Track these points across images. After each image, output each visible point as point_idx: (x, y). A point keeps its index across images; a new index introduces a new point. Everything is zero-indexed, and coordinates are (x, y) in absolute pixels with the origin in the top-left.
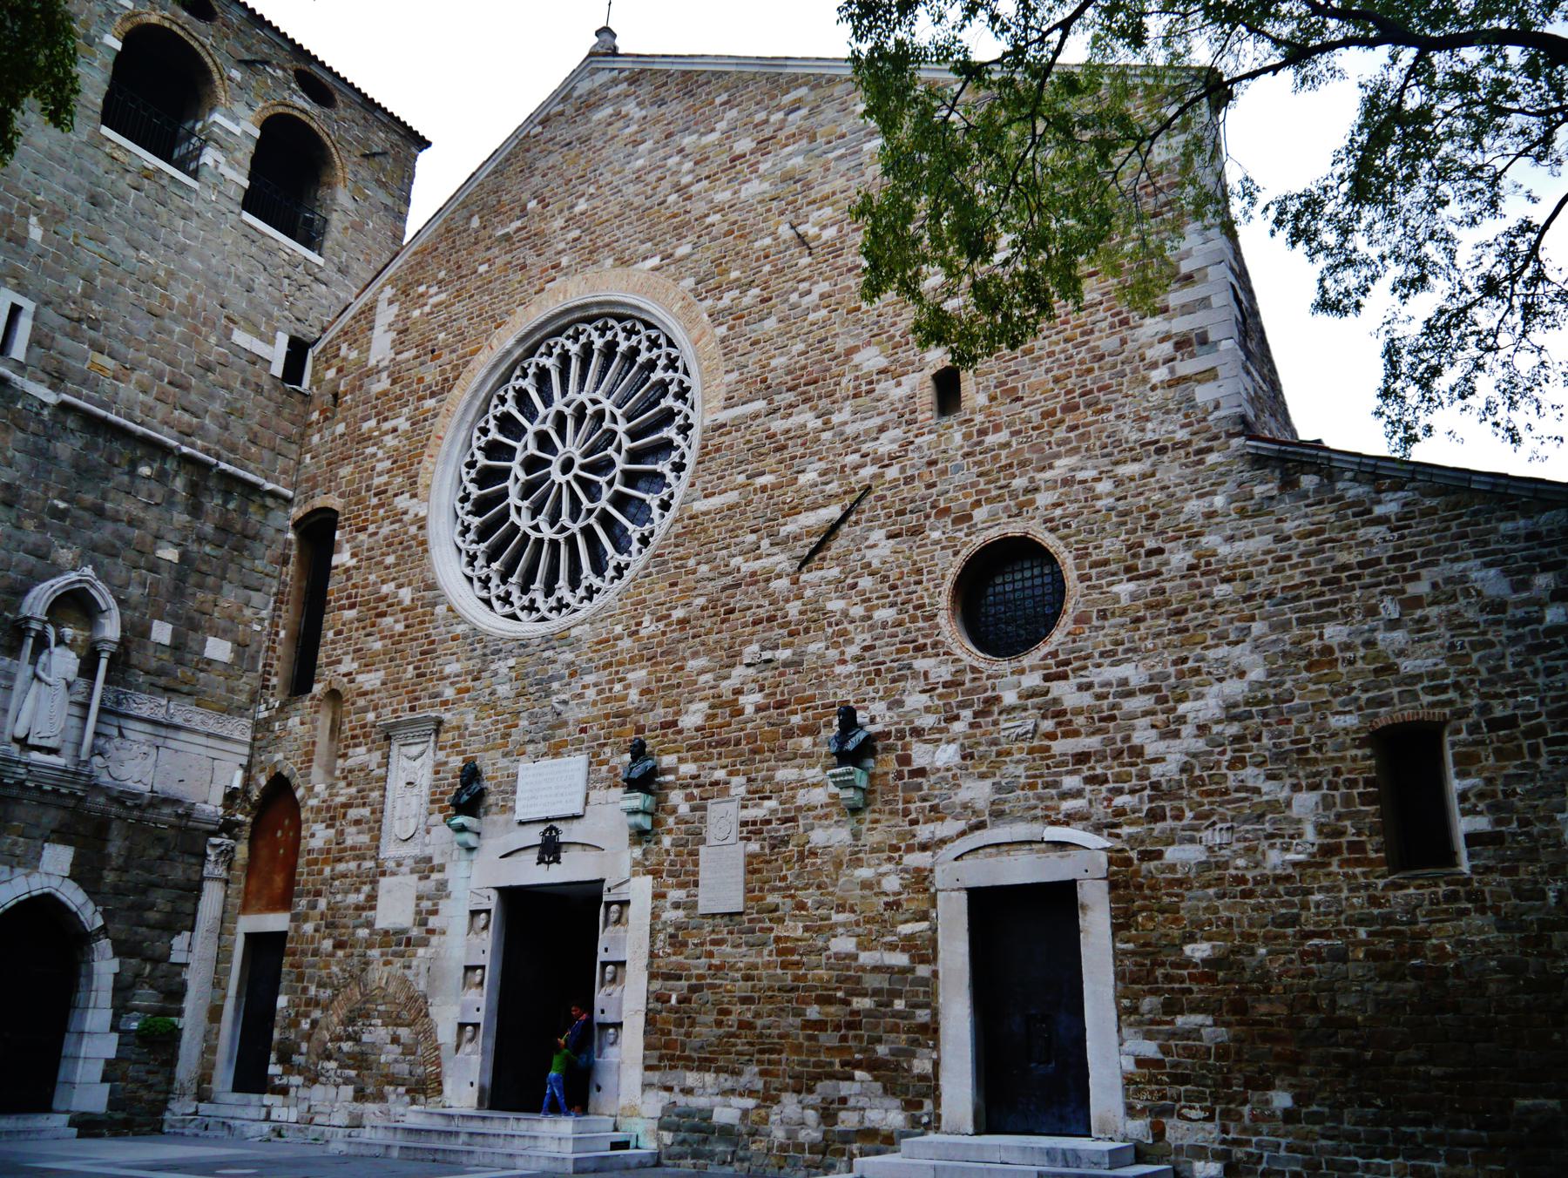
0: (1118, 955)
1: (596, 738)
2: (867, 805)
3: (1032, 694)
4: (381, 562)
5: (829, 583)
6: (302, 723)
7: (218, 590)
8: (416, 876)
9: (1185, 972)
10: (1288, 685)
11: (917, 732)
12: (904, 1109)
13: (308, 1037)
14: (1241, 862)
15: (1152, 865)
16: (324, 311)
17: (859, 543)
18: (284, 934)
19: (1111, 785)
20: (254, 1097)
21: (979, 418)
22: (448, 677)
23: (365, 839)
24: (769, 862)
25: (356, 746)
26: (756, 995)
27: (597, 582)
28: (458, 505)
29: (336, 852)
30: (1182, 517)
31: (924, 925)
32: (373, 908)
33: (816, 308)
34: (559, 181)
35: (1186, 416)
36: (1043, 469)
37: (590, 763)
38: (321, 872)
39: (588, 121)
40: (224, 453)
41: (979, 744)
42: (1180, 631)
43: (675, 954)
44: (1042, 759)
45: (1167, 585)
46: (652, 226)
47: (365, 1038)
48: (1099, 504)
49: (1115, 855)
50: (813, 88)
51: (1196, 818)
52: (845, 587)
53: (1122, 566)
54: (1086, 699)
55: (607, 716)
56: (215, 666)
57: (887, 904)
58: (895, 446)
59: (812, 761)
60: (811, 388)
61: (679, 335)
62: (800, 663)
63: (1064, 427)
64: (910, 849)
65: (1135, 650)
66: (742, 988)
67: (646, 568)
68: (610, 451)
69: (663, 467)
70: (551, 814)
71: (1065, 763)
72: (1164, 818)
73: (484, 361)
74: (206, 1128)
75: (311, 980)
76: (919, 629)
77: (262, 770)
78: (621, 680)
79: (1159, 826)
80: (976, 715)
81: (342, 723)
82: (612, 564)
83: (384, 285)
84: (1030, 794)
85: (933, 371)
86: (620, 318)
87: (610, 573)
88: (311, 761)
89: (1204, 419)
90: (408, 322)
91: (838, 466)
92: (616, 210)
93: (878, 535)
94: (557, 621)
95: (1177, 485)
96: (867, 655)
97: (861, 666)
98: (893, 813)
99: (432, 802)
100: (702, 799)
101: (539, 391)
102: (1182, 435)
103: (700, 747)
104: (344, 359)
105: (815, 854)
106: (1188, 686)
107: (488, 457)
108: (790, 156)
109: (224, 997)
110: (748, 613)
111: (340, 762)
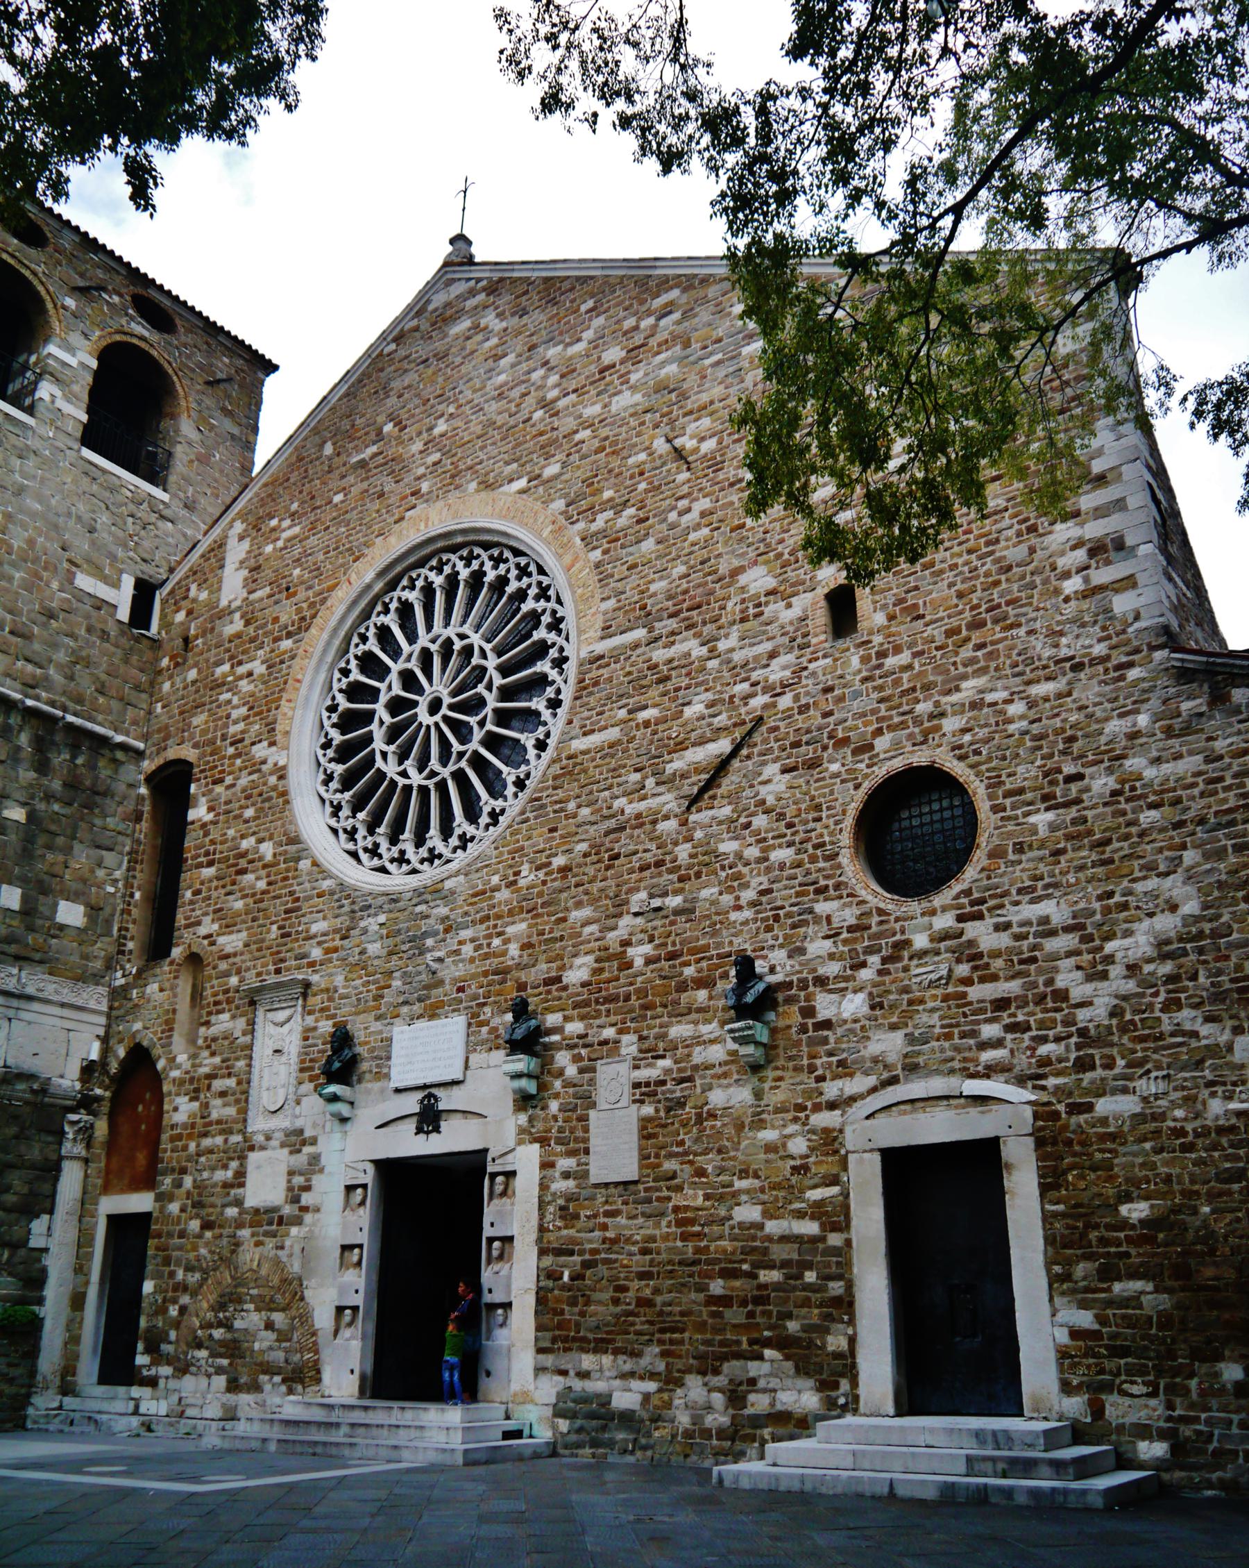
0: (1047, 1218)
1: (475, 997)
2: (769, 1061)
3: (945, 936)
4: (240, 816)
5: (720, 823)
6: (161, 990)
7: (68, 851)
8: (286, 1151)
9: (1122, 1235)
10: (1225, 919)
11: (821, 981)
12: (819, 1390)
13: (177, 1324)
14: (1179, 1113)
15: (1082, 1118)
16: (172, 550)
17: (752, 779)
18: (147, 1216)
19: (1034, 1033)
20: (121, 1390)
21: (877, 639)
22: (315, 936)
23: (231, 1111)
24: (664, 1126)
25: (219, 1012)
26: (655, 1270)
27: (470, 830)
28: (320, 752)
29: (201, 1127)
30: (1103, 739)
31: (835, 1190)
32: (242, 1185)
33: (697, 527)
34: (417, 401)
36: (949, 692)
37: (469, 1025)
38: (185, 1148)
40: (70, 705)
41: (888, 992)
42: (1104, 863)
43: (566, 1227)
44: (958, 1006)
45: (1089, 814)
47: (238, 1324)
48: (1012, 728)
49: (1040, 1109)
51: (1128, 1066)
52: (739, 827)
53: (1038, 794)
55: (486, 974)
56: (67, 931)
57: (793, 1168)
58: (788, 673)
59: (708, 1015)
60: (695, 613)
61: (550, 562)
62: (693, 911)
63: (970, 645)
64: (817, 1108)
65: (1056, 885)
66: (640, 1262)
67: (523, 813)
68: (480, 689)
69: (538, 704)
70: (428, 1081)
71: (984, 1011)
72: (1093, 1068)
73: (341, 598)
74: (72, 1423)
75: (178, 1264)
76: (819, 870)
77: (121, 1041)
78: (499, 934)
79: (1088, 1077)
80: (885, 961)
81: (203, 989)
82: (486, 809)
83: (233, 520)
84: (947, 1044)
85: (826, 591)
86: (486, 546)
87: (484, 819)
88: (171, 1030)
90: (261, 559)
91: (726, 696)
92: (478, 430)
93: (772, 770)
94: (430, 873)
95: (1095, 705)
96: (764, 899)
97: (758, 912)
98: (797, 1069)
99: (302, 1070)
101: (402, 627)
103: (586, 1004)
104: (194, 600)
106: (1115, 923)
107: (350, 700)
109: (87, 1283)
110: (635, 858)
111: (203, 1030)
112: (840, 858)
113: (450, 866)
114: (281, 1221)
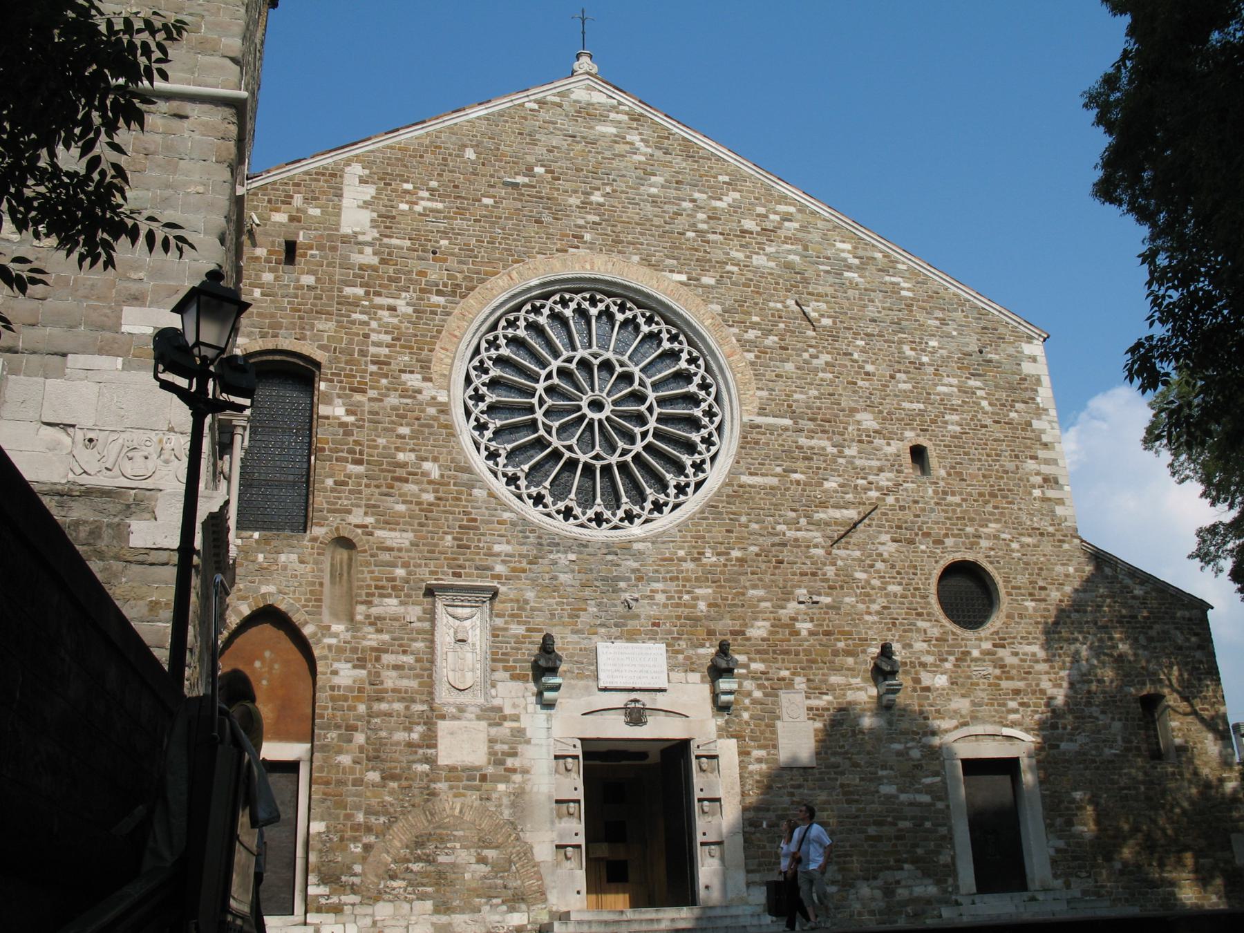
0: (1043, 796)
1: (670, 632)
3: (988, 653)
4: (393, 430)
8: (484, 724)
11: (923, 665)
14: (1094, 752)
21: (942, 484)
22: (498, 555)
23: (413, 684)
25: (382, 596)
31: (938, 779)
32: (435, 746)
35: (1053, 520)
36: (982, 526)
38: (354, 708)
39: (592, 128)
46: (677, 248)
47: (442, 859)
48: (1015, 555)
50: (799, 211)
54: (1014, 661)
55: (679, 618)
57: (914, 766)
58: (890, 484)
60: (827, 424)
62: (839, 608)
67: (702, 512)
70: (637, 686)
71: (1008, 694)
75: (357, 807)
76: (918, 603)
77: (244, 598)
78: (688, 592)
80: (957, 660)
84: (992, 708)
88: (320, 600)
89: (1059, 525)
93: (885, 538)
96: (885, 612)
97: (881, 618)
99: (494, 660)
102: (1051, 529)
103: (766, 652)
105: (863, 733)
108: (789, 252)
111: (361, 609)
112: (929, 599)
113: (614, 533)
114: (484, 778)
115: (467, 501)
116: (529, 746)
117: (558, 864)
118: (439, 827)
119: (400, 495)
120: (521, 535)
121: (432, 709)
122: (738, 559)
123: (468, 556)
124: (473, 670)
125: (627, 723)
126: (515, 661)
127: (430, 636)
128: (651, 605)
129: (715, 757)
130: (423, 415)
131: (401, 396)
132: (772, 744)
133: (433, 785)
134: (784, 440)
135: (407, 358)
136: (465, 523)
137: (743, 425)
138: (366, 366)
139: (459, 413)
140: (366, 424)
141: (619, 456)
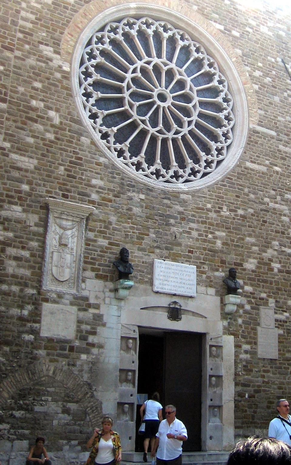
1: (198, 258)
4: (30, 83)
8: (75, 308)
22: (94, 186)
23: (28, 273)
25: (10, 203)
32: (39, 322)
47: (37, 408)
55: (205, 249)
70: (177, 293)
78: (211, 233)
99: (85, 262)
100: (256, 304)
103: (254, 280)
108: (280, 29)
110: (273, 226)
113: (167, 184)
114: (72, 349)
115: (77, 144)
116: (104, 328)
117: (118, 416)
118: (37, 384)
119: (31, 131)
120: (110, 175)
121: (39, 293)
122: (242, 216)
123: (74, 184)
124: (70, 268)
125: (169, 318)
126: (99, 265)
127: (42, 238)
128: (189, 238)
129: (221, 347)
130: (52, 77)
131: (38, 60)
132: (254, 342)
133: (35, 352)
134: (271, 144)
135: (44, 34)
136: (73, 159)
137: (250, 130)
138: (15, 32)
139: (75, 82)
140: (11, 74)
141: (174, 134)
